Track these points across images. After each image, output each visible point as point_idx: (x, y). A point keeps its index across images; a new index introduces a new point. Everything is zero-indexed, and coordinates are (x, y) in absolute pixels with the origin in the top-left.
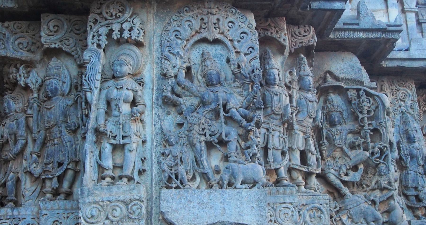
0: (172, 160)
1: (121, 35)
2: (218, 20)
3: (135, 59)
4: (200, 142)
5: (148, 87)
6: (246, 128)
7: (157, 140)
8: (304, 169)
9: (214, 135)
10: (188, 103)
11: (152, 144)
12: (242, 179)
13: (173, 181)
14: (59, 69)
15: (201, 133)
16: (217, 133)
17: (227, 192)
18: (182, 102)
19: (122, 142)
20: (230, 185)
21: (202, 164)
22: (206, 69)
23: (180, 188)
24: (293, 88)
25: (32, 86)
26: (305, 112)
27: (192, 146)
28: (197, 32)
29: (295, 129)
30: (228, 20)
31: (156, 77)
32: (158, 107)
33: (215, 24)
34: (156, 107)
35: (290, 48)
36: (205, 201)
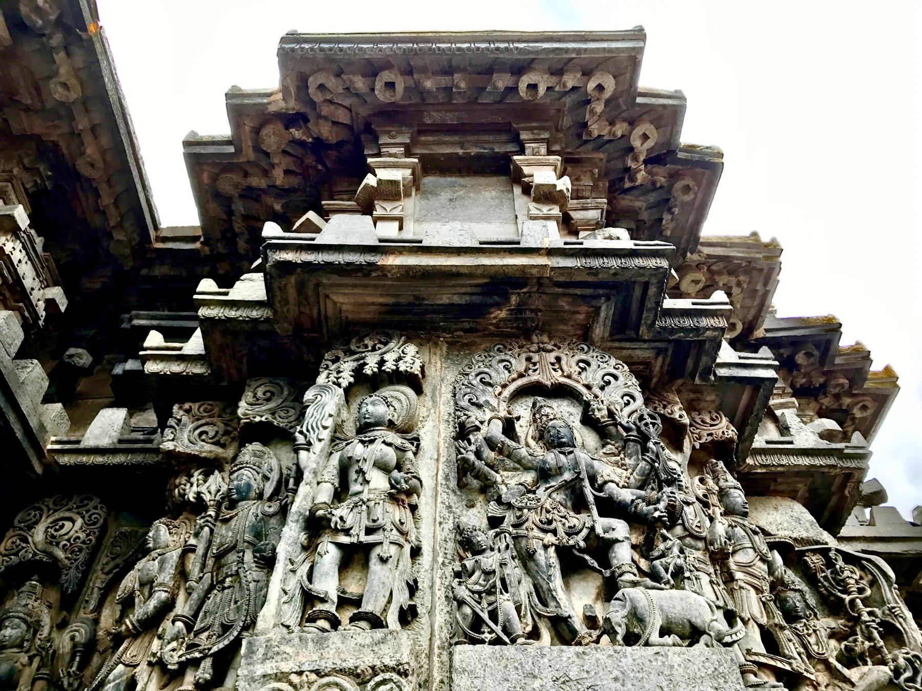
0: (481, 581)
1: (379, 368)
2: (558, 359)
3: (404, 403)
4: (546, 547)
5: (428, 455)
6: (650, 517)
7: (446, 551)
8: (779, 665)
9: (577, 534)
10: (512, 482)
11: (434, 560)
12: (660, 623)
13: (484, 626)
14: (260, 457)
15: (546, 526)
16: (581, 530)
17: (628, 654)
18: (499, 479)
19: (364, 539)
20: (631, 639)
21: (554, 598)
22: (544, 418)
23: (505, 644)
24: (713, 505)
25: (207, 497)
26: (748, 549)
27: (526, 558)
28: (521, 376)
29: (737, 580)
30: (577, 358)
31: (445, 443)
32: (447, 491)
33: (553, 364)
34: (444, 492)
35: (690, 441)
36: (573, 674)
